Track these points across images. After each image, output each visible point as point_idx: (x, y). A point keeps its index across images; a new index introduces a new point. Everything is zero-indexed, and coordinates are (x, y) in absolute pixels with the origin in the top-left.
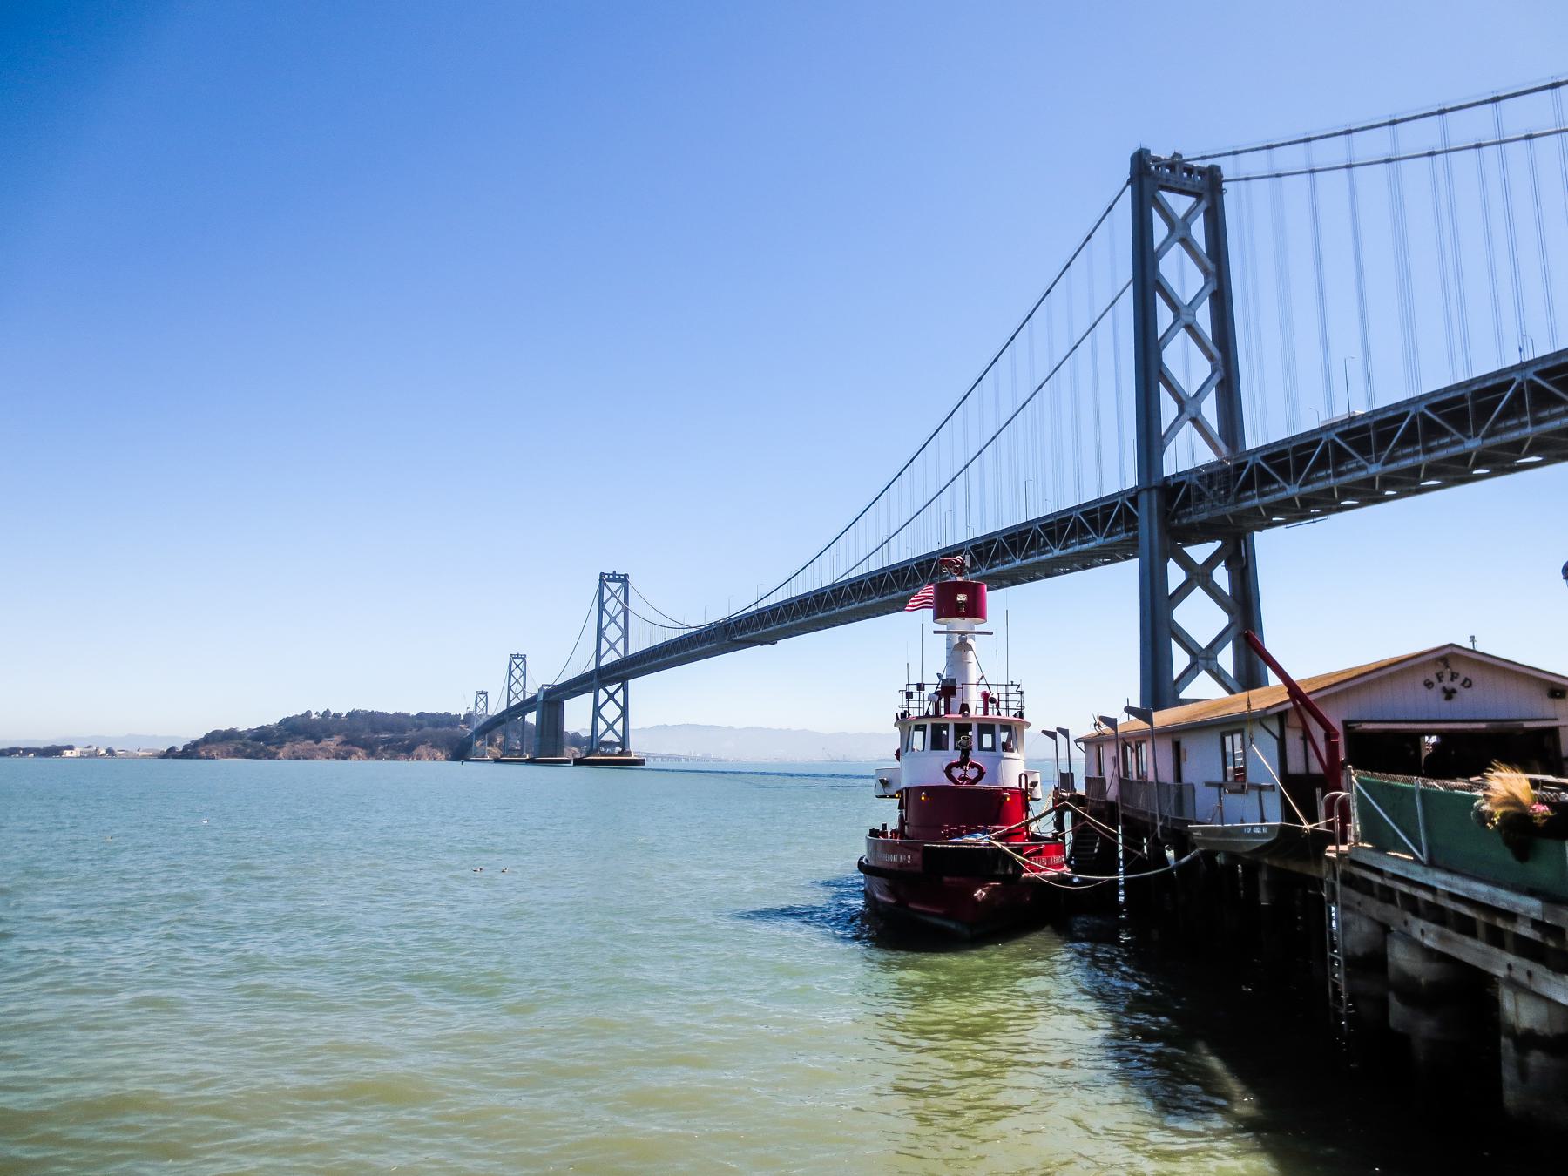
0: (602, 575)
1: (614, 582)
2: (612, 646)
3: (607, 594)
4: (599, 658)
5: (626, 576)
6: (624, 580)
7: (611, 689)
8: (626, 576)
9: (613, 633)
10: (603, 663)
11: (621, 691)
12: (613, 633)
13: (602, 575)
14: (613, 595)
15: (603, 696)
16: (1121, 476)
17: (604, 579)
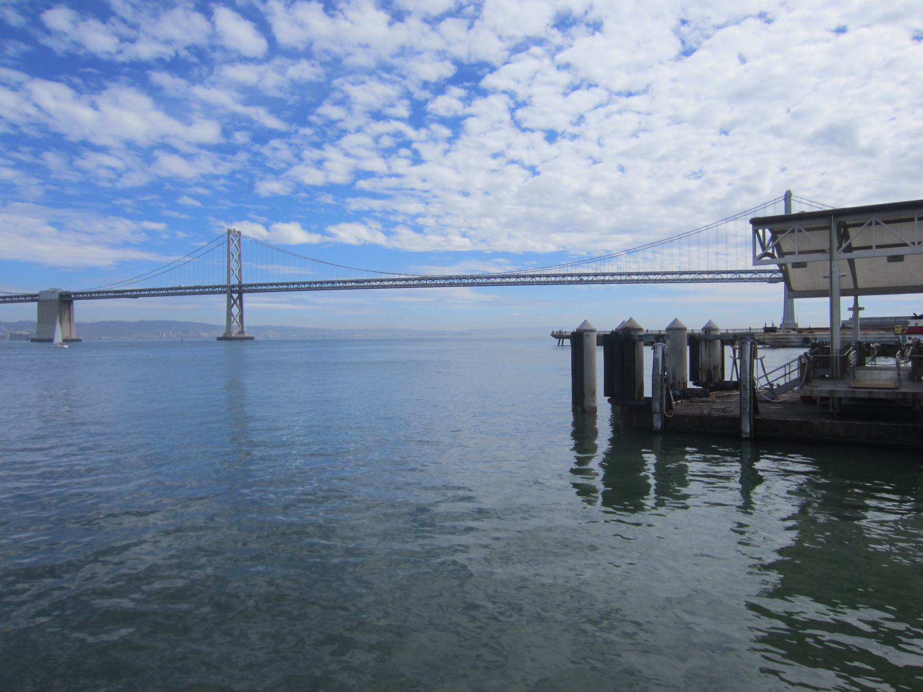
16: (224, 282)
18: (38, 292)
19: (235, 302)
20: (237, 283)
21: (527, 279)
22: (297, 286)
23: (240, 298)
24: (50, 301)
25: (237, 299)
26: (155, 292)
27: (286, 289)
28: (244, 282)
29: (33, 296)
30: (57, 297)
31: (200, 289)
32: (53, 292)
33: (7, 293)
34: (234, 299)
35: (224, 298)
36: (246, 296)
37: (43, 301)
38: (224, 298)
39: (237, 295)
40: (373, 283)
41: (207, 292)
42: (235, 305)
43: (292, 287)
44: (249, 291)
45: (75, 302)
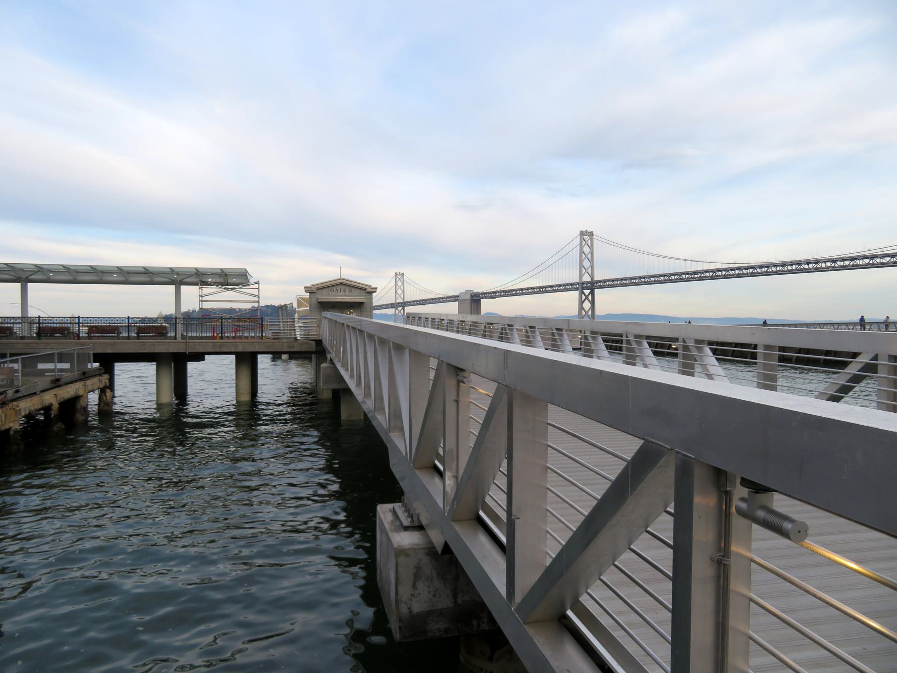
0: (396, 273)
1: (399, 276)
2: (399, 296)
3: (398, 279)
4: (396, 299)
5: (403, 273)
6: (403, 275)
7: (400, 309)
8: (403, 273)
9: (400, 292)
10: (397, 302)
11: (403, 310)
12: (400, 292)
13: (396, 273)
14: (400, 279)
15: (397, 311)
17: (396, 274)
18: (458, 294)
19: (587, 298)
20: (589, 279)
21: (763, 269)
22: (766, 269)
23: (592, 293)
24: (465, 300)
25: (589, 295)
26: (628, 282)
27: (752, 273)
28: (596, 279)
29: (455, 296)
30: (468, 297)
31: (666, 277)
32: (467, 292)
33: (442, 294)
34: (585, 295)
35: (576, 294)
36: (596, 290)
37: (461, 300)
38: (576, 294)
39: (590, 291)
40: (858, 262)
41: (672, 280)
42: (587, 300)
43: (759, 270)
44: (601, 287)
45: (482, 300)
